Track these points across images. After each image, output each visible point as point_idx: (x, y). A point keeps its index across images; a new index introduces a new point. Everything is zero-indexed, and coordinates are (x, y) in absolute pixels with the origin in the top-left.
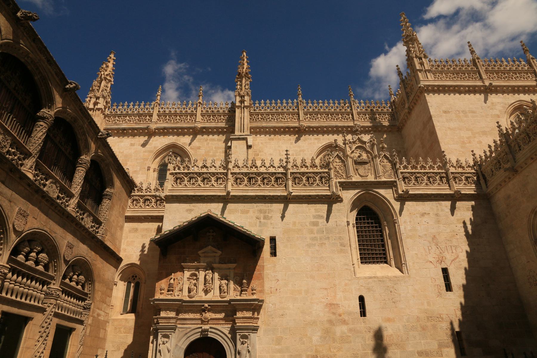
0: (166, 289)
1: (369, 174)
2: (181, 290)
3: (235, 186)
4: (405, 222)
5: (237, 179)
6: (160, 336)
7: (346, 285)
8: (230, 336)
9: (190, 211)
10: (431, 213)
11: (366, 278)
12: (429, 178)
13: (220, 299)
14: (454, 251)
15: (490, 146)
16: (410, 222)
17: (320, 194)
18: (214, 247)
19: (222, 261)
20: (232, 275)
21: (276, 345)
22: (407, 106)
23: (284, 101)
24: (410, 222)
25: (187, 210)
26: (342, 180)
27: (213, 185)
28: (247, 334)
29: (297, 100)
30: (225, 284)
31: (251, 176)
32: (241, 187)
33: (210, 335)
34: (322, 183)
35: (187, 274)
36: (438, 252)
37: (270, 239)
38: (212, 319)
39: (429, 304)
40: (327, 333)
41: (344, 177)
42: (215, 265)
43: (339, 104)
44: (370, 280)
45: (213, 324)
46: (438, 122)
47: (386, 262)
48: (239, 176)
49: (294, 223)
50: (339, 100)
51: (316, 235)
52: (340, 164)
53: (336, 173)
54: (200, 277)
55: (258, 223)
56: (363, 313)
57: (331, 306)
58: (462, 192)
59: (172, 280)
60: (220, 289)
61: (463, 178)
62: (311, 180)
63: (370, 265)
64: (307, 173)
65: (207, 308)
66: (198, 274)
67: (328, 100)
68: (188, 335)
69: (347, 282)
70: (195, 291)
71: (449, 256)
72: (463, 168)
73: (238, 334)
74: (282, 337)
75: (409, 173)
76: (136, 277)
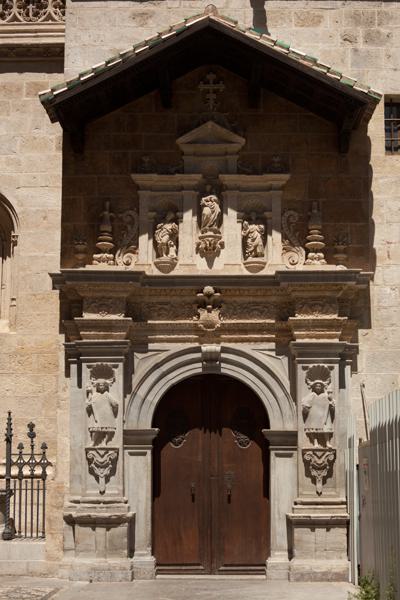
9: (144, 17)
13: (246, 273)
18: (223, 126)
19: (247, 166)
20: (277, 206)
25: (134, 16)
28: (326, 366)
42: (227, 179)
45: (230, 341)
60: (245, 245)
68: (164, 368)
73: (300, 366)
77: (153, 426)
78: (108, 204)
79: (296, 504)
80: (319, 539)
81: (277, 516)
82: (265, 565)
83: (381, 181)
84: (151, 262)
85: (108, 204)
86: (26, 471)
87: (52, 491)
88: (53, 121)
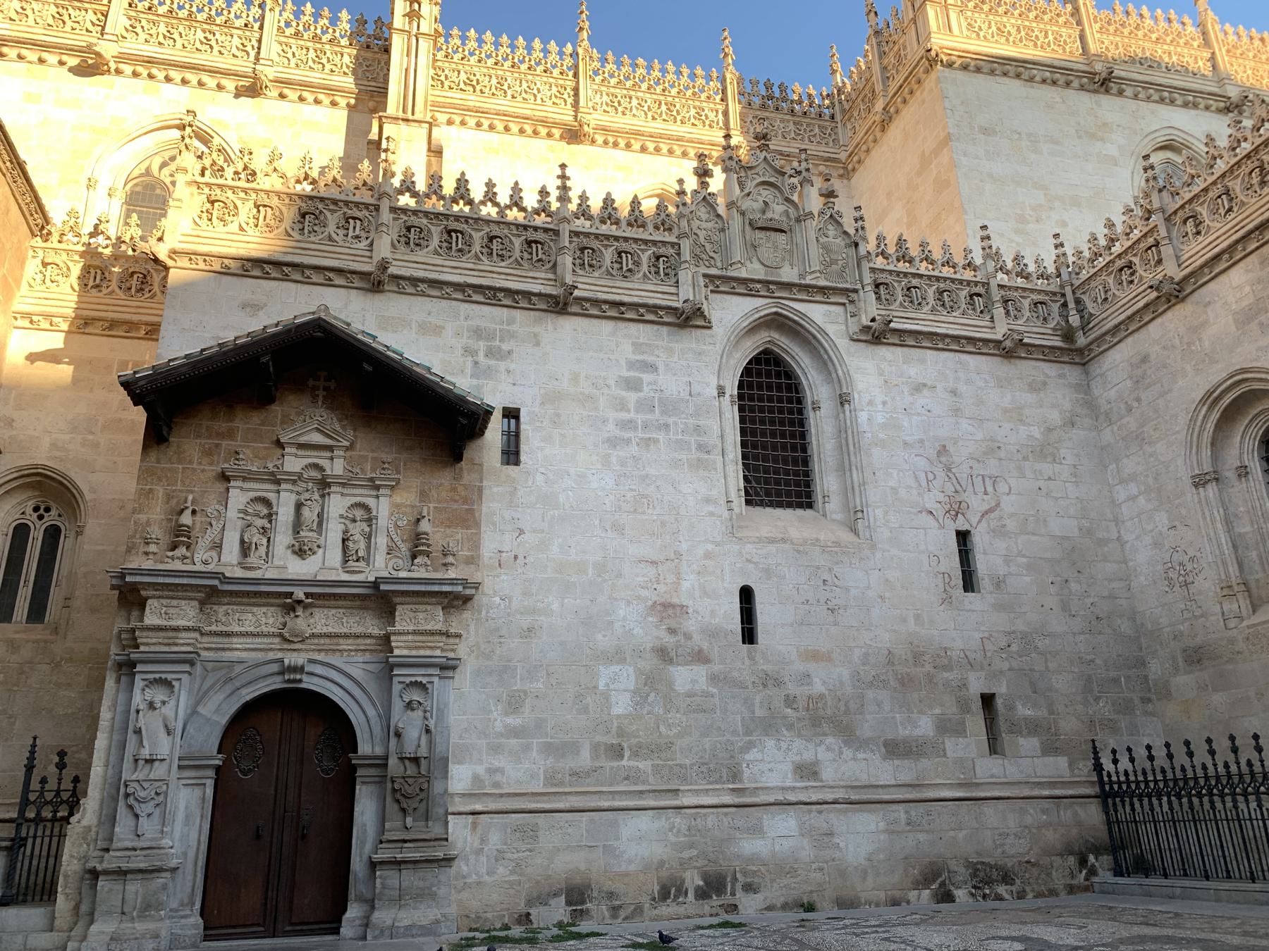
0: (165, 540)
1: (787, 264)
2: (218, 546)
3: (402, 248)
4: (870, 403)
5: (408, 229)
6: (139, 683)
7: (708, 555)
8: (372, 687)
9: (252, 307)
10: (939, 386)
11: (760, 540)
12: (941, 292)
14: (990, 489)
15: (1110, 225)
16: (884, 403)
17: (651, 302)
21: (506, 714)
22: (879, 106)
23: (537, 44)
24: (884, 403)
26: (713, 271)
27: (330, 238)
28: (424, 680)
29: (574, 46)
30: (363, 534)
31: (454, 225)
32: (421, 255)
33: (309, 683)
34: (657, 273)
35: (238, 497)
36: (949, 489)
37: (504, 416)
38: (313, 636)
39: (918, 618)
40: (651, 683)
41: (719, 264)
43: (693, 76)
44: (772, 548)
45: (319, 650)
46: (965, 155)
47: (810, 506)
48: (414, 220)
49: (575, 378)
50: (691, 67)
51: (632, 415)
52: (710, 225)
53: (698, 251)
54: (281, 511)
55: (469, 364)
56: (749, 636)
57: (667, 610)
58: (1026, 340)
59: (188, 512)
61: (1026, 303)
62: (627, 262)
63: (769, 510)
64: (617, 238)
65: (299, 602)
66: (274, 502)
67: (663, 63)
69: (710, 547)
70: (262, 550)
71: (976, 503)
72: (1027, 277)
73: (396, 680)
74: (525, 693)
75: (891, 272)
76: (47, 510)
77: (219, 752)
78: (190, 497)
79: (381, 842)
80: (404, 884)
81: (358, 859)
82: (340, 921)
83: (495, 490)
84: (235, 562)
85: (190, 497)
86: (47, 813)
87: (75, 836)
88: (135, 405)
